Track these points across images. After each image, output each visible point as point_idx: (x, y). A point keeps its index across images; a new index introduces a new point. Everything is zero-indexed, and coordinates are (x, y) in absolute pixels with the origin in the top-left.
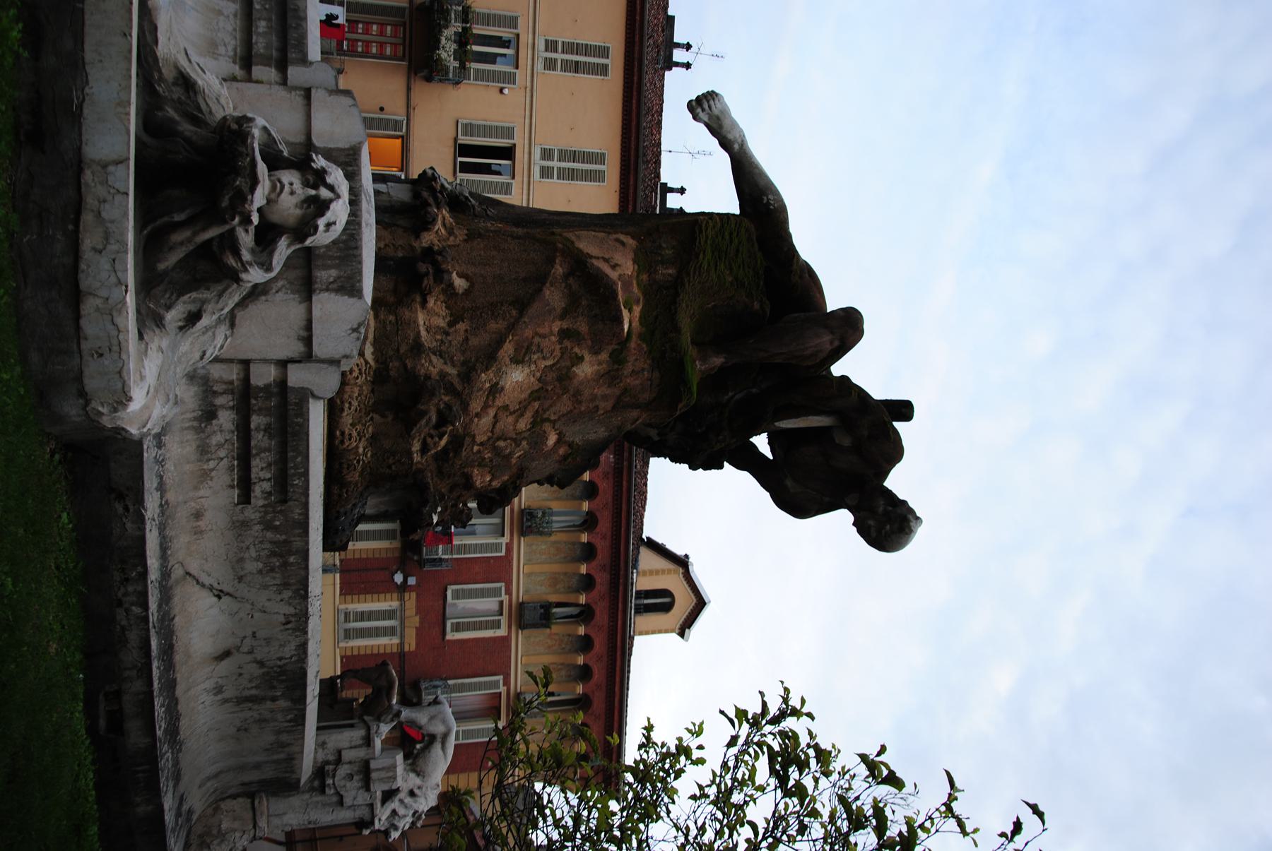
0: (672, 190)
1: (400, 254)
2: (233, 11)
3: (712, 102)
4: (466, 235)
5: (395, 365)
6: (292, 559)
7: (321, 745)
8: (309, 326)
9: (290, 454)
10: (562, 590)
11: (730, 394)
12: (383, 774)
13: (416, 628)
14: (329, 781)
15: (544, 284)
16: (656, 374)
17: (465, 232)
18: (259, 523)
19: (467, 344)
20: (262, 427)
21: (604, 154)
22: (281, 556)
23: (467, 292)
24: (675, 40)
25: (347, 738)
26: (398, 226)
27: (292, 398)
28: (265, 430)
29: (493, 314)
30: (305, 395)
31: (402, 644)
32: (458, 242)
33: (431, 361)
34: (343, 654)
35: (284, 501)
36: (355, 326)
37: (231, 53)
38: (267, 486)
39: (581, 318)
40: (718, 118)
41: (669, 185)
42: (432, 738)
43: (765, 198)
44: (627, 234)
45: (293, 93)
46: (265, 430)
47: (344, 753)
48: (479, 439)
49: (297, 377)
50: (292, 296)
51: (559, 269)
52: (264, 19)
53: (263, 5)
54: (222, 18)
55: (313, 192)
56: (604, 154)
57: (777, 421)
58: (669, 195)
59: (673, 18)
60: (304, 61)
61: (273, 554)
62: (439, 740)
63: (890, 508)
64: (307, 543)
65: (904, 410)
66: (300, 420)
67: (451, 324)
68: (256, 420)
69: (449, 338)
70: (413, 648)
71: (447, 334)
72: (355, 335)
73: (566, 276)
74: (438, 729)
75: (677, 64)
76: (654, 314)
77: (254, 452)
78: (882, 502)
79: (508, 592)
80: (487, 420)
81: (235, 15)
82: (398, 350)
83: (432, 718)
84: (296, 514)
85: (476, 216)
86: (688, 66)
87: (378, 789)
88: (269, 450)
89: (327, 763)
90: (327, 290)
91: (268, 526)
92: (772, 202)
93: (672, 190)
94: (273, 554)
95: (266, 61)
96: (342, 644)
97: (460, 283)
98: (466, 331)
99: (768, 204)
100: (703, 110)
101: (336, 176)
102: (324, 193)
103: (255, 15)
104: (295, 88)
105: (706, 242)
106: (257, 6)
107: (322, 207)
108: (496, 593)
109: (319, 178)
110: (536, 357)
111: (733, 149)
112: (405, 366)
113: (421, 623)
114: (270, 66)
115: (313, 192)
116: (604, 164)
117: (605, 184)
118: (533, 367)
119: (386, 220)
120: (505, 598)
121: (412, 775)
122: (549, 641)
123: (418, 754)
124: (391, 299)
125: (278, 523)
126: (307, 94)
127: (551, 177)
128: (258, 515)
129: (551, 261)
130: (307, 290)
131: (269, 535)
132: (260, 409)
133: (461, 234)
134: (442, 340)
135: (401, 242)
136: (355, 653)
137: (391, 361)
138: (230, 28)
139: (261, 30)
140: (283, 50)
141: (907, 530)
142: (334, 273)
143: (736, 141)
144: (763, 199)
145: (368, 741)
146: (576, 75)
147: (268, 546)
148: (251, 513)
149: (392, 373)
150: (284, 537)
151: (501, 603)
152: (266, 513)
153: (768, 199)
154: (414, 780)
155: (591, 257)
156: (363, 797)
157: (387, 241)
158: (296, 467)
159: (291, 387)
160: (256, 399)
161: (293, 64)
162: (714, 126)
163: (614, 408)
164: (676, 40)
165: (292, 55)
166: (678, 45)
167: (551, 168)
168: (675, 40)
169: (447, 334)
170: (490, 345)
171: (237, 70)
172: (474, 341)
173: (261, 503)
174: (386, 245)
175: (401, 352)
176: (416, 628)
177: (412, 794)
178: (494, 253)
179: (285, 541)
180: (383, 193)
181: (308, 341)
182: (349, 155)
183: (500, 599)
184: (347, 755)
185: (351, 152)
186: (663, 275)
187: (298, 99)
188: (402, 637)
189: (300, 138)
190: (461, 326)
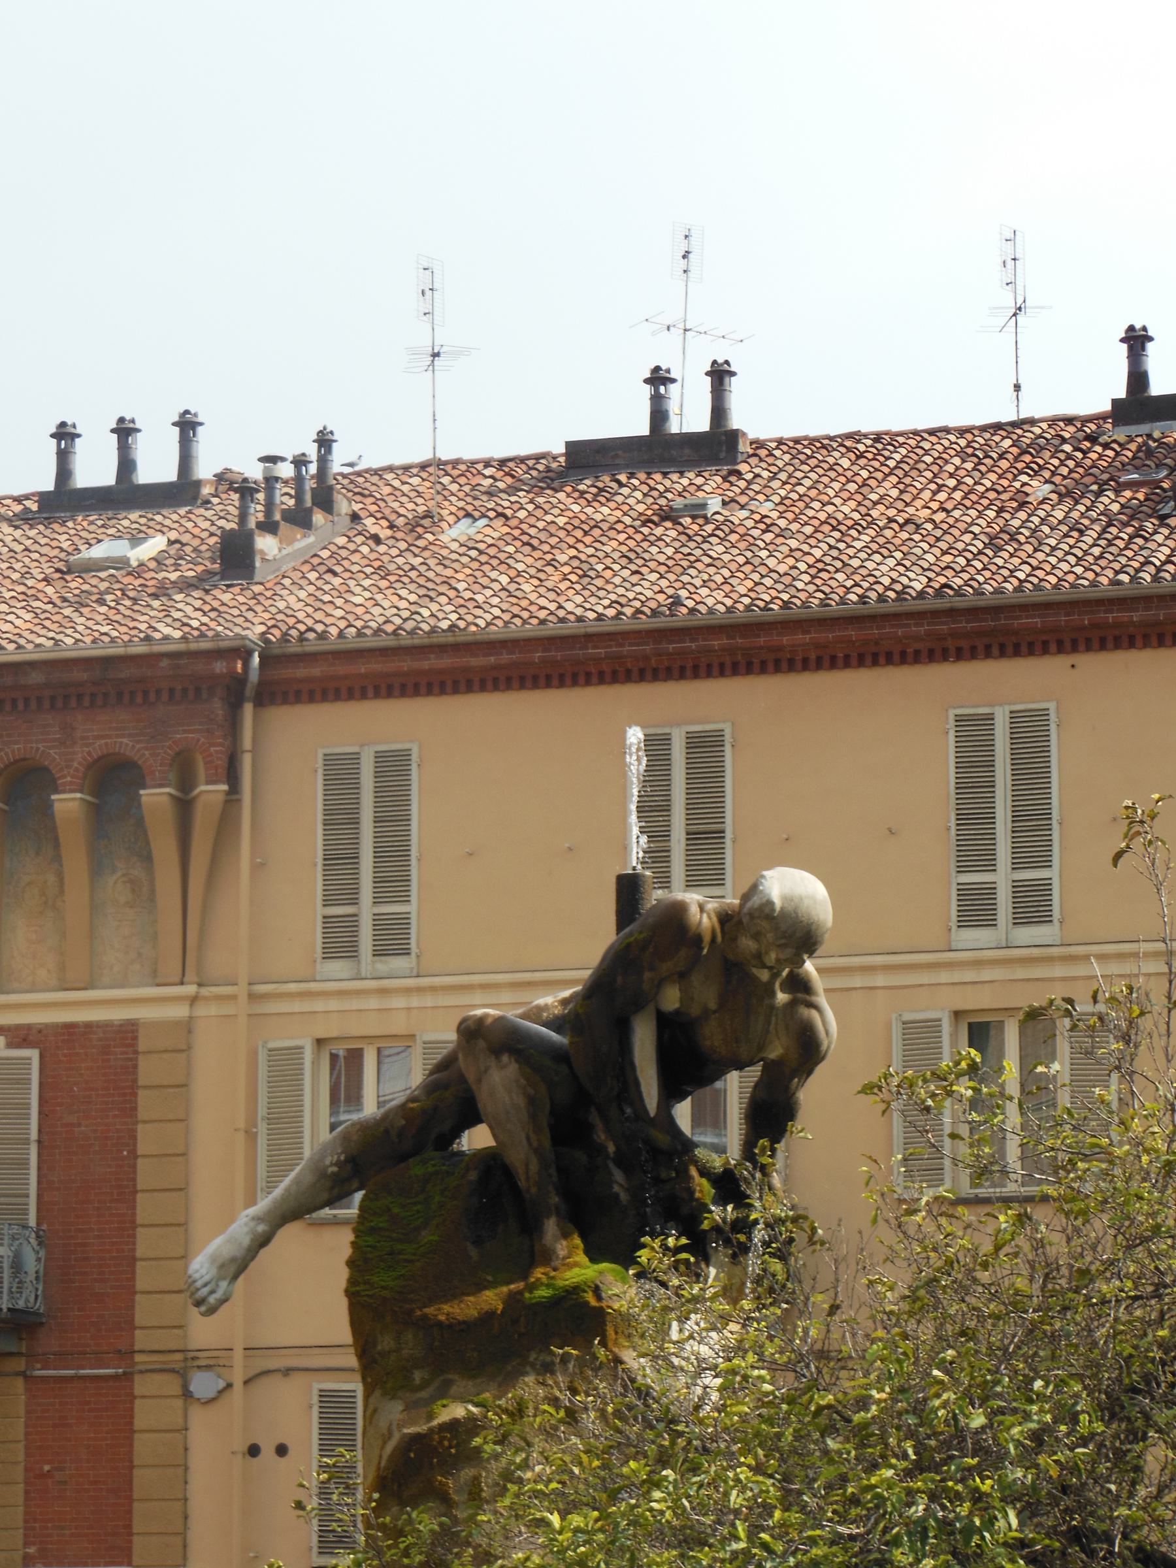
0: (1138, 378)
3: (199, 1284)
21: (959, 719)
24: (645, 431)
40: (222, 1266)
41: (1122, 393)
56: (959, 719)
59: (569, 445)
75: (719, 412)
86: (720, 375)
92: (336, 1157)
93: (1138, 378)
99: (338, 1164)
100: (212, 1292)
116: (990, 717)
117: (1052, 706)
127: (1045, 887)
144: (333, 1173)
146: (729, 835)
153: (332, 1164)
162: (232, 1269)
164: (642, 428)
166: (659, 415)
167: (1018, 889)
168: (645, 431)
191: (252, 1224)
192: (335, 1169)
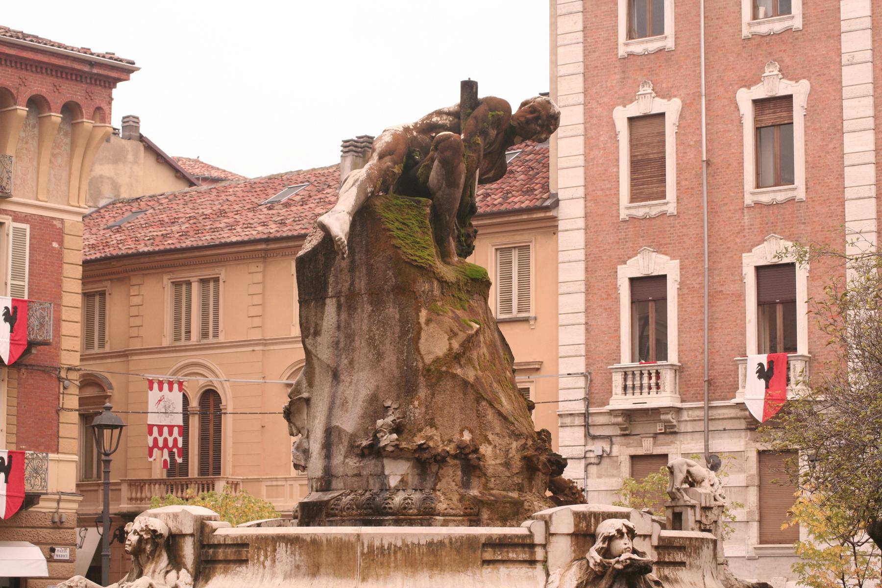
1: (459, 473)
2: (504, 569)
4: (431, 428)
7: (693, 529)
12: (708, 500)
14: (708, 527)
17: (428, 428)
23: (471, 431)
25: (690, 517)
26: (437, 473)
30: (660, 538)
32: (438, 434)
37: (531, 570)
42: (688, 472)
44: (418, 315)
47: (697, 519)
54: (511, 574)
55: (626, 535)
58: (560, 347)
62: (689, 468)
63: (540, 122)
65: (469, 87)
67: (490, 443)
68: (667, 560)
73: (461, 366)
74: (685, 468)
81: (508, 568)
82: (509, 477)
83: (681, 471)
85: (404, 417)
87: (713, 503)
89: (700, 527)
95: (533, 553)
102: (625, 530)
103: (505, 558)
104: (546, 538)
105: (419, 257)
106: (500, 558)
112: (517, 473)
115: (626, 535)
119: (432, 480)
121: (703, 484)
123: (693, 479)
124: (483, 480)
129: (454, 376)
135: (451, 472)
138: (516, 570)
139: (515, 556)
140: (523, 545)
145: (693, 507)
148: (688, 563)
149: (520, 481)
154: (706, 483)
156: (715, 511)
157: (451, 480)
161: (533, 541)
165: (528, 541)
171: (539, 567)
172: (498, 430)
174: (453, 481)
175: (509, 475)
177: (712, 485)
178: (445, 411)
184: (698, 518)
187: (553, 540)
189: (569, 538)
190: (490, 437)
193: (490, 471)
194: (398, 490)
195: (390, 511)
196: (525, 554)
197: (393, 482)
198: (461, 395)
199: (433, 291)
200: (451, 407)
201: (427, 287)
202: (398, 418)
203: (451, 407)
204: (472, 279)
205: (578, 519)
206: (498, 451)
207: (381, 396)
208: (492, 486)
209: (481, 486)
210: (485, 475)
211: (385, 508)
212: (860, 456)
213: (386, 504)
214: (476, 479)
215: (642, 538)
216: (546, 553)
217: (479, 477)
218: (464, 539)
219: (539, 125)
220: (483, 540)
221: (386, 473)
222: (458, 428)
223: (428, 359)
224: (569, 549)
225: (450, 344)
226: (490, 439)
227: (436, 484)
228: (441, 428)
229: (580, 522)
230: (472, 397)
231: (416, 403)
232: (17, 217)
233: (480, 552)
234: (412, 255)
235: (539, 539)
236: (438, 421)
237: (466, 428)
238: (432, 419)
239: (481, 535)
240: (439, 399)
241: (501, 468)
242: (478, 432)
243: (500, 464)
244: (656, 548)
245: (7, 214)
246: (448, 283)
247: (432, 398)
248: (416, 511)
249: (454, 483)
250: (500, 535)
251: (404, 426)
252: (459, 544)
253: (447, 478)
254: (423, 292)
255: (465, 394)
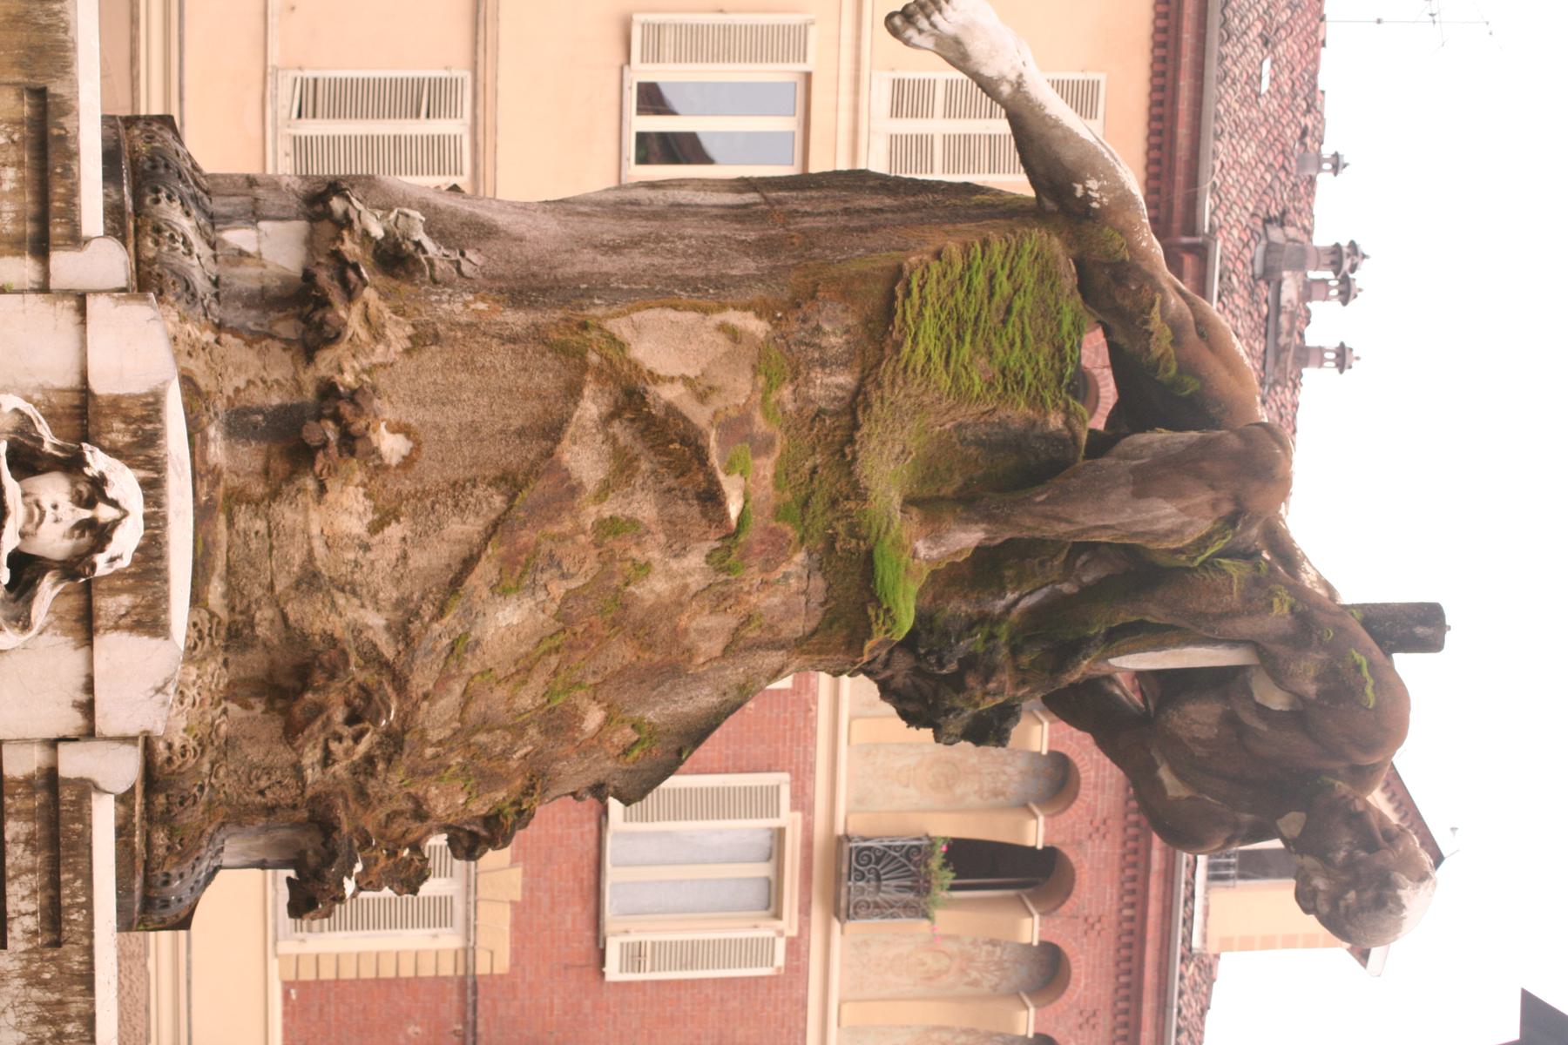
1: (275, 400)
3: (936, 17)
4: (410, 338)
5: (263, 616)
6: (70, 1028)
8: (89, 687)
9: (64, 877)
10: (973, 800)
11: (1010, 597)
13: (513, 903)
15: (557, 441)
16: (818, 583)
17: (409, 330)
18: (20, 976)
19: (405, 564)
20: (22, 838)
22: (52, 1022)
23: (408, 462)
26: (272, 337)
27: (67, 795)
28: (27, 843)
29: (456, 505)
30: (86, 788)
31: (468, 953)
32: (392, 356)
33: (333, 603)
34: (292, 977)
35: (57, 944)
36: (160, 684)
38: (30, 923)
39: (639, 496)
43: (1079, 187)
44: (746, 308)
45: (59, 305)
46: (27, 843)
48: (434, 735)
49: (73, 763)
50: (63, 639)
51: (590, 408)
52: (13, 165)
53: (9, 137)
55: (86, 514)
57: (1112, 657)
60: (76, 240)
61: (42, 1020)
63: (1362, 854)
64: (92, 1004)
66: (78, 826)
67: (376, 527)
69: (370, 556)
70: (503, 965)
71: (366, 548)
72: (160, 697)
73: (607, 420)
76: (809, 464)
77: (10, 873)
78: (1348, 839)
79: (802, 801)
80: (447, 704)
82: (271, 587)
84: (76, 961)
85: (435, 282)
88: (32, 870)
90: (116, 627)
91: (34, 980)
92: (1096, 195)
94: (42, 1020)
96: (289, 947)
97: (392, 446)
98: (404, 539)
100: (921, 31)
101: (124, 483)
102: (105, 513)
104: (66, 293)
105: (920, 314)
107: (100, 534)
108: (764, 802)
109: (95, 491)
110: (546, 576)
111: (1001, 93)
112: (285, 617)
113: (529, 888)
114: (21, 255)
115: (86, 514)
118: (541, 596)
119: (250, 324)
120: (789, 819)
122: (928, 958)
124: (258, 489)
125: (47, 976)
126: (80, 300)
128: (18, 964)
129: (573, 392)
130: (86, 626)
131: (36, 993)
132: (18, 812)
133: (398, 333)
134: (356, 561)
135: (276, 375)
136: (327, 974)
137: (259, 608)
140: (43, 218)
141: (1391, 905)
142: (126, 600)
143: (1002, 79)
144: (1075, 189)
147: (33, 1008)
149: (260, 631)
150: (57, 996)
151: (779, 834)
152: (30, 961)
153: (1086, 189)
155: (656, 378)
158: (74, 895)
159: (68, 781)
160: (12, 796)
161: (58, 247)
163: (726, 649)
165: (57, 230)
169: (366, 548)
170: (449, 566)
172: (418, 560)
173: (22, 946)
174: (250, 382)
175: (278, 589)
176: (513, 903)
178: (463, 377)
179: (60, 1003)
180: (249, 255)
181: (88, 708)
182: (148, 404)
183: (774, 823)
185: (151, 400)
186: (827, 386)
187: (65, 312)
188: (470, 928)
189: (70, 380)
190: (394, 531)
191: (1013, 77)
192: (1079, 192)
193: (286, 514)
194: (213, 246)
195: (148, 201)
196: (15, 221)
197: (237, 237)
198: (516, 423)
199: (823, 364)
200: (478, 392)
201: (835, 341)
202: (431, 262)
203: (478, 392)
204: (869, 554)
205: (137, 412)
206: (350, 556)
207: (494, 246)
208: (241, 524)
209: (237, 482)
210: (275, 495)
211: (157, 191)
212: (429, 752)
213: (169, 198)
214: (258, 463)
215: (83, 697)
216: (21, 292)
217: (266, 472)
218: (61, 36)
219: (1350, 855)
220: (55, 88)
221: (263, 225)
222: (414, 417)
223: (620, 327)
224: (34, 382)
225: (672, 380)
226: (388, 531)
227: (235, 332)
228: (412, 364)
229: (127, 419)
230: (515, 456)
231: (481, 306)
232: (796, 948)
233: (18, 79)
234: (921, 288)
235: (66, 266)
236: (432, 357)
237: (417, 447)
238: (437, 338)
239: (74, 84)
240: (501, 358)
241: (298, 558)
242: (407, 486)
243: (311, 551)
244: (51, 777)
245: (800, 928)
246: (851, 441)
247: (501, 337)
248: (151, 254)
249: (242, 385)
250: (76, 138)
251: (410, 277)
252: (43, 20)
253: (258, 363)
254: (818, 329)
255: (520, 433)
